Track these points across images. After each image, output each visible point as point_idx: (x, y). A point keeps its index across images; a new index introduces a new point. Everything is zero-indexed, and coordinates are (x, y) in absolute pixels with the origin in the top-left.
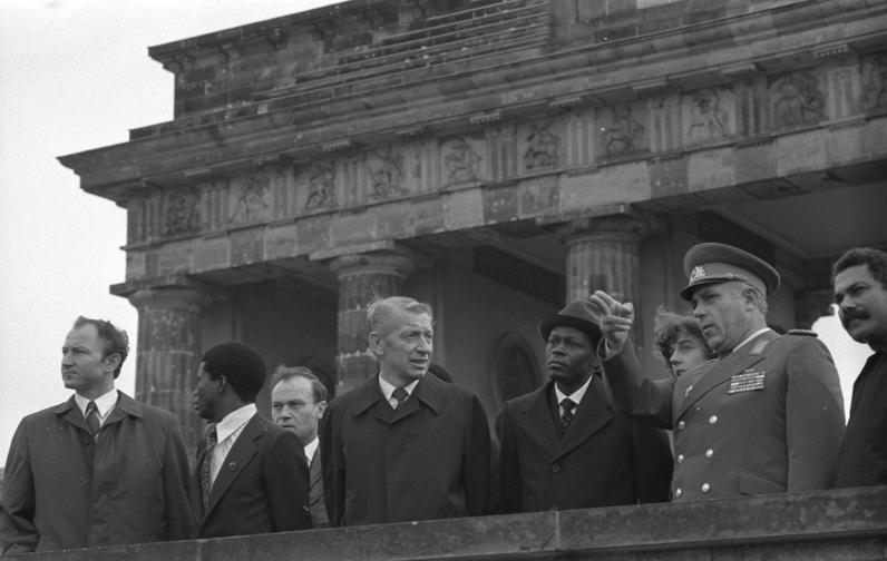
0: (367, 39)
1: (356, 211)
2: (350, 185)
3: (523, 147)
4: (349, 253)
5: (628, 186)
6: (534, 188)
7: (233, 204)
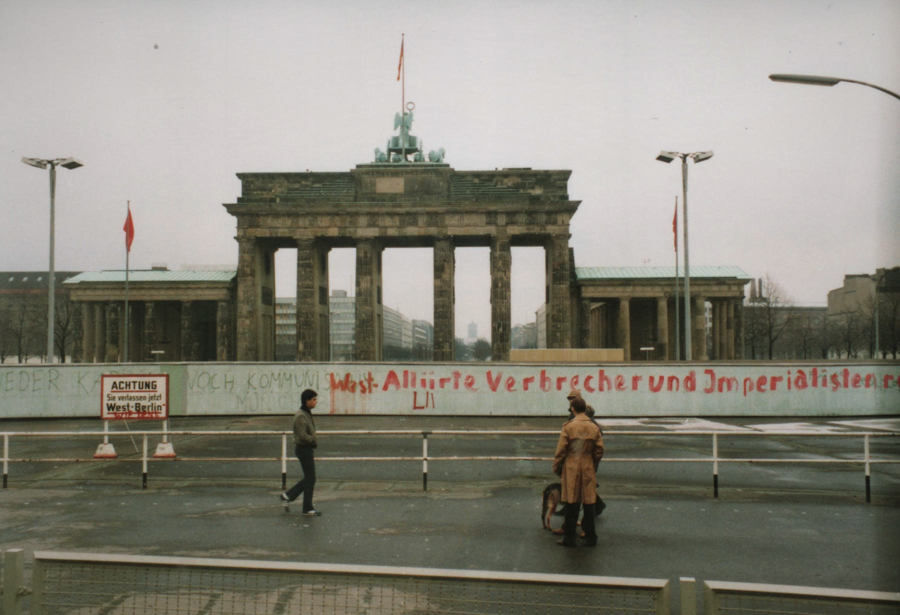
0: (299, 182)
1: (305, 228)
2: (301, 222)
3: (348, 220)
4: (305, 238)
5: (372, 232)
6: (351, 230)
7: (270, 221)
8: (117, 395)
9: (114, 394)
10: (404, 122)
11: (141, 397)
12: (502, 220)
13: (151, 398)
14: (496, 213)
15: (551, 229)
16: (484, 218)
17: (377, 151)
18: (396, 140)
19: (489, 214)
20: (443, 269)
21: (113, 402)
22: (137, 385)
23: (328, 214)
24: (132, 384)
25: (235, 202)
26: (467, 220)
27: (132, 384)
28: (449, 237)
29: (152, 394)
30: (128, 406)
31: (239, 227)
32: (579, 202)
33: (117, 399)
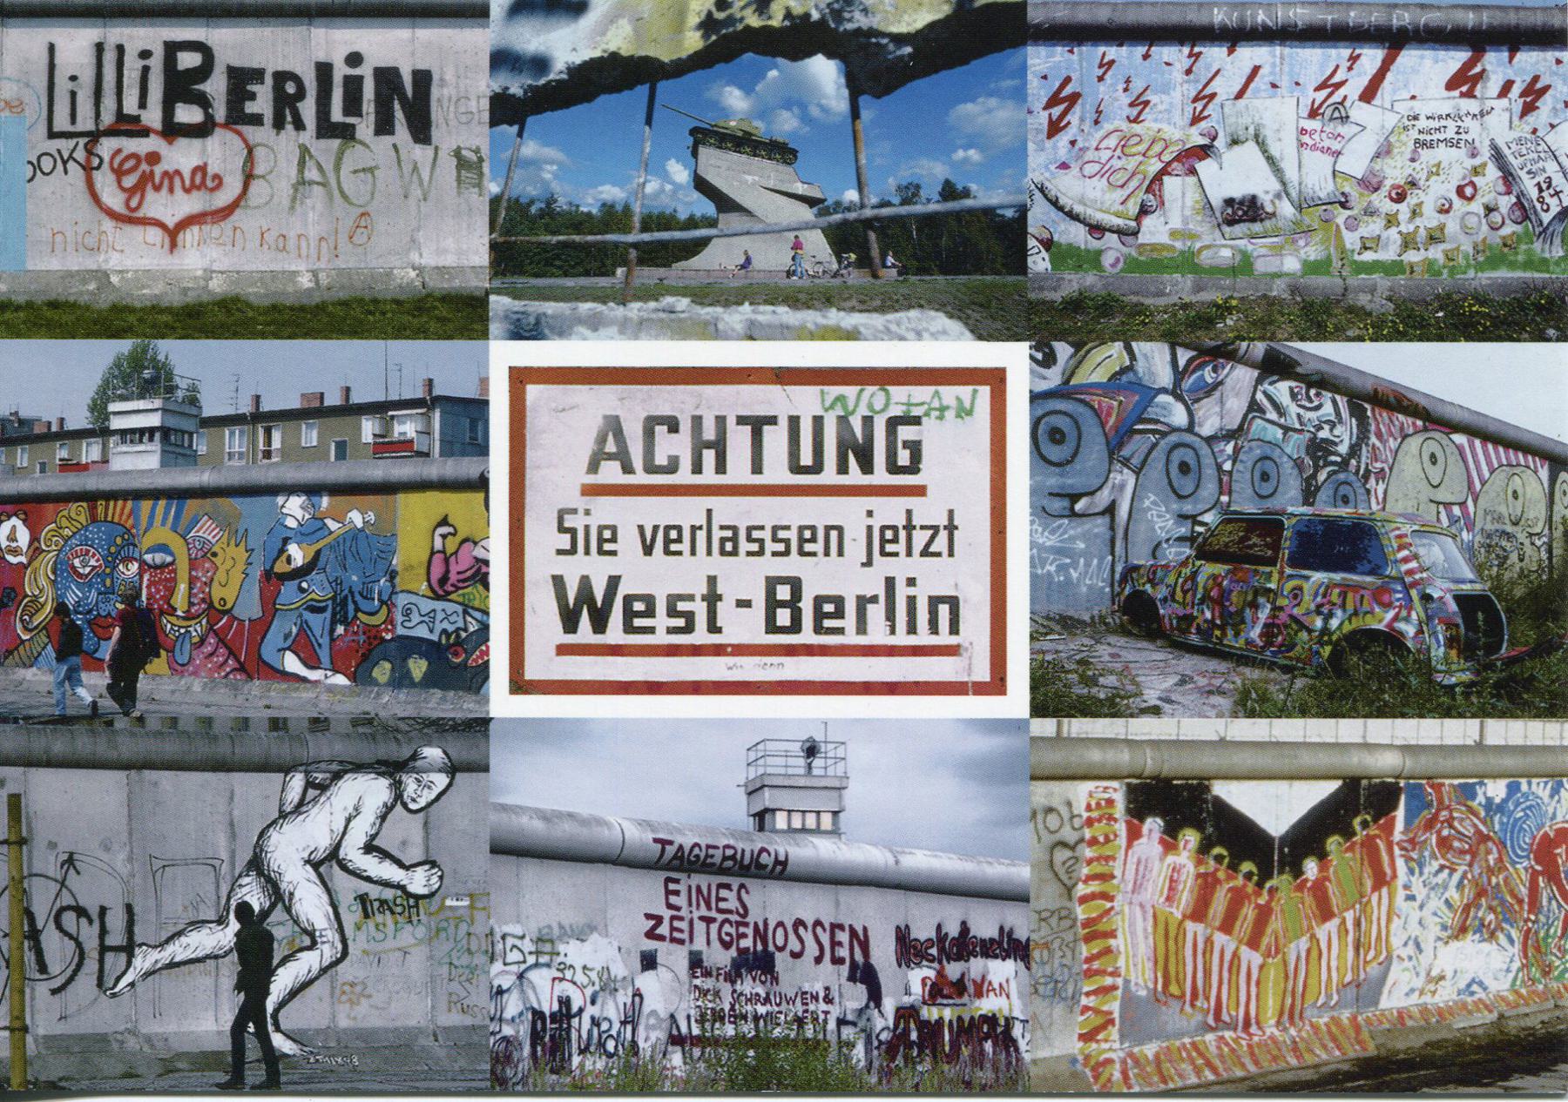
8: (629, 515)
9: (607, 510)
11: (807, 535)
13: (883, 541)
21: (598, 571)
22: (776, 440)
24: (739, 441)
27: (739, 441)
29: (891, 511)
30: (712, 599)
33: (629, 542)
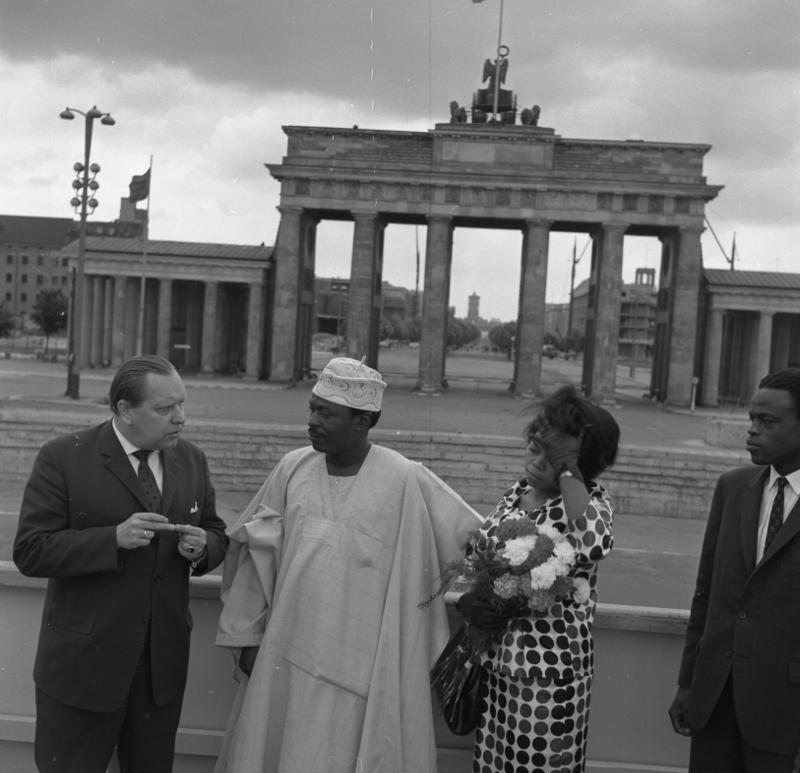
2: (362, 192)
3: (422, 193)
5: (453, 210)
10: (495, 71)
12: (618, 204)
14: (611, 195)
15: (680, 220)
16: (594, 203)
17: (454, 106)
18: (483, 94)
19: (602, 196)
20: (533, 261)
23: (397, 184)
25: (279, 162)
26: (572, 202)
28: (549, 222)
31: (282, 195)
32: (721, 187)
